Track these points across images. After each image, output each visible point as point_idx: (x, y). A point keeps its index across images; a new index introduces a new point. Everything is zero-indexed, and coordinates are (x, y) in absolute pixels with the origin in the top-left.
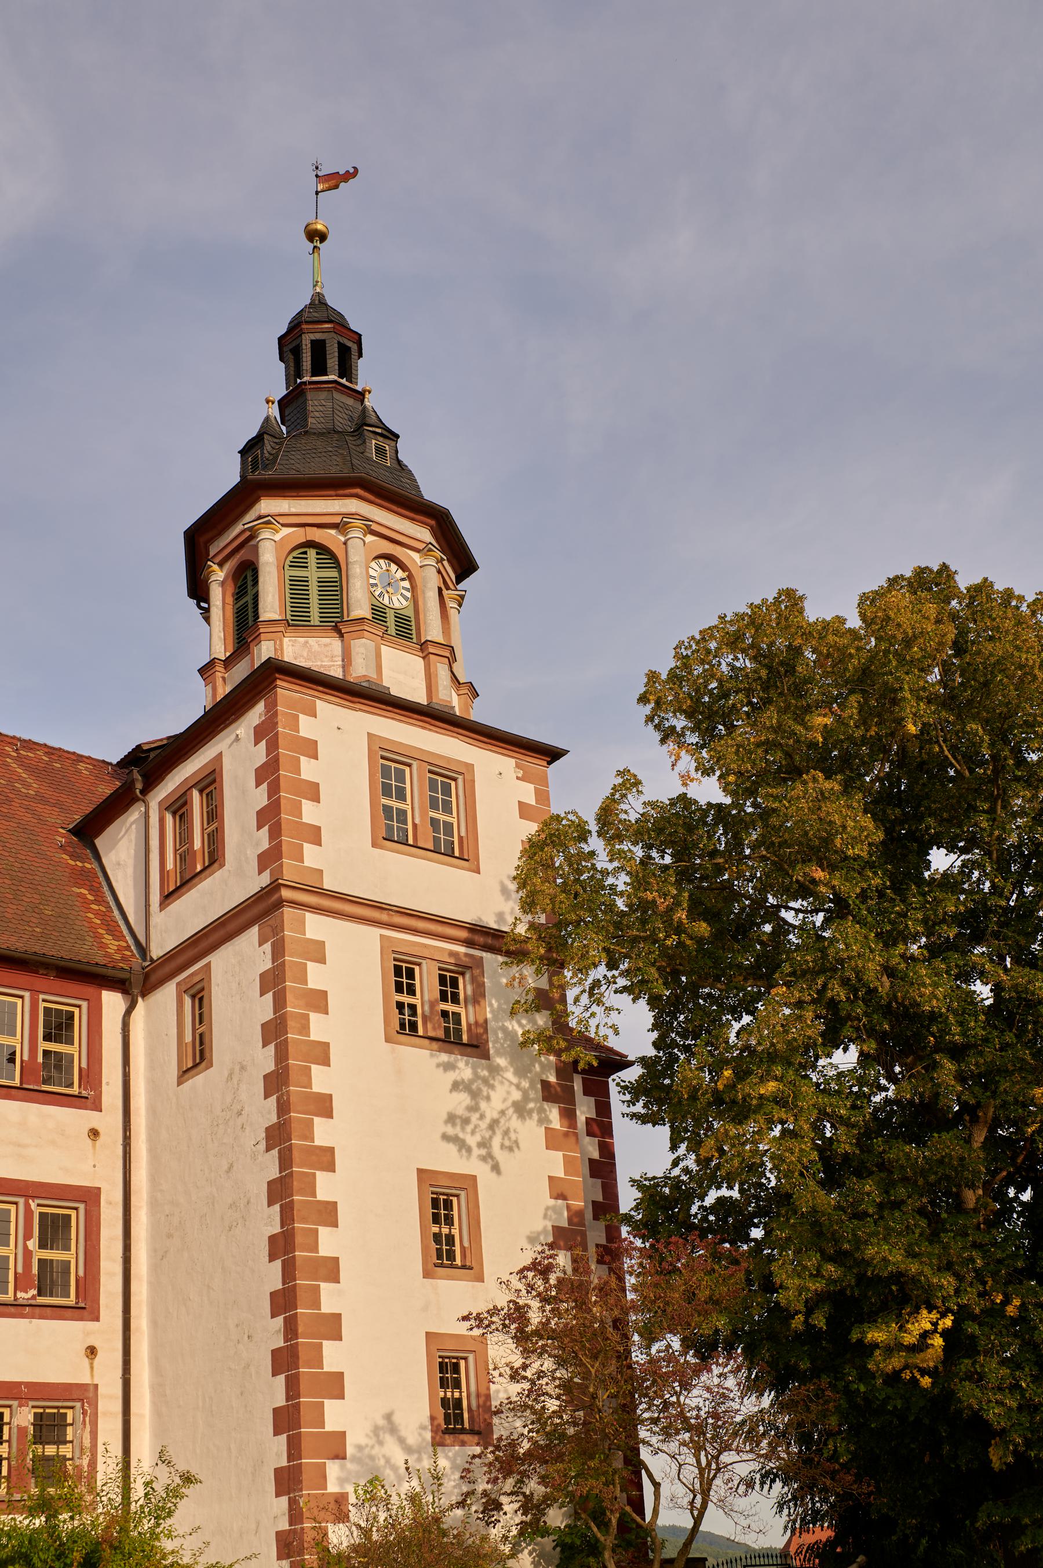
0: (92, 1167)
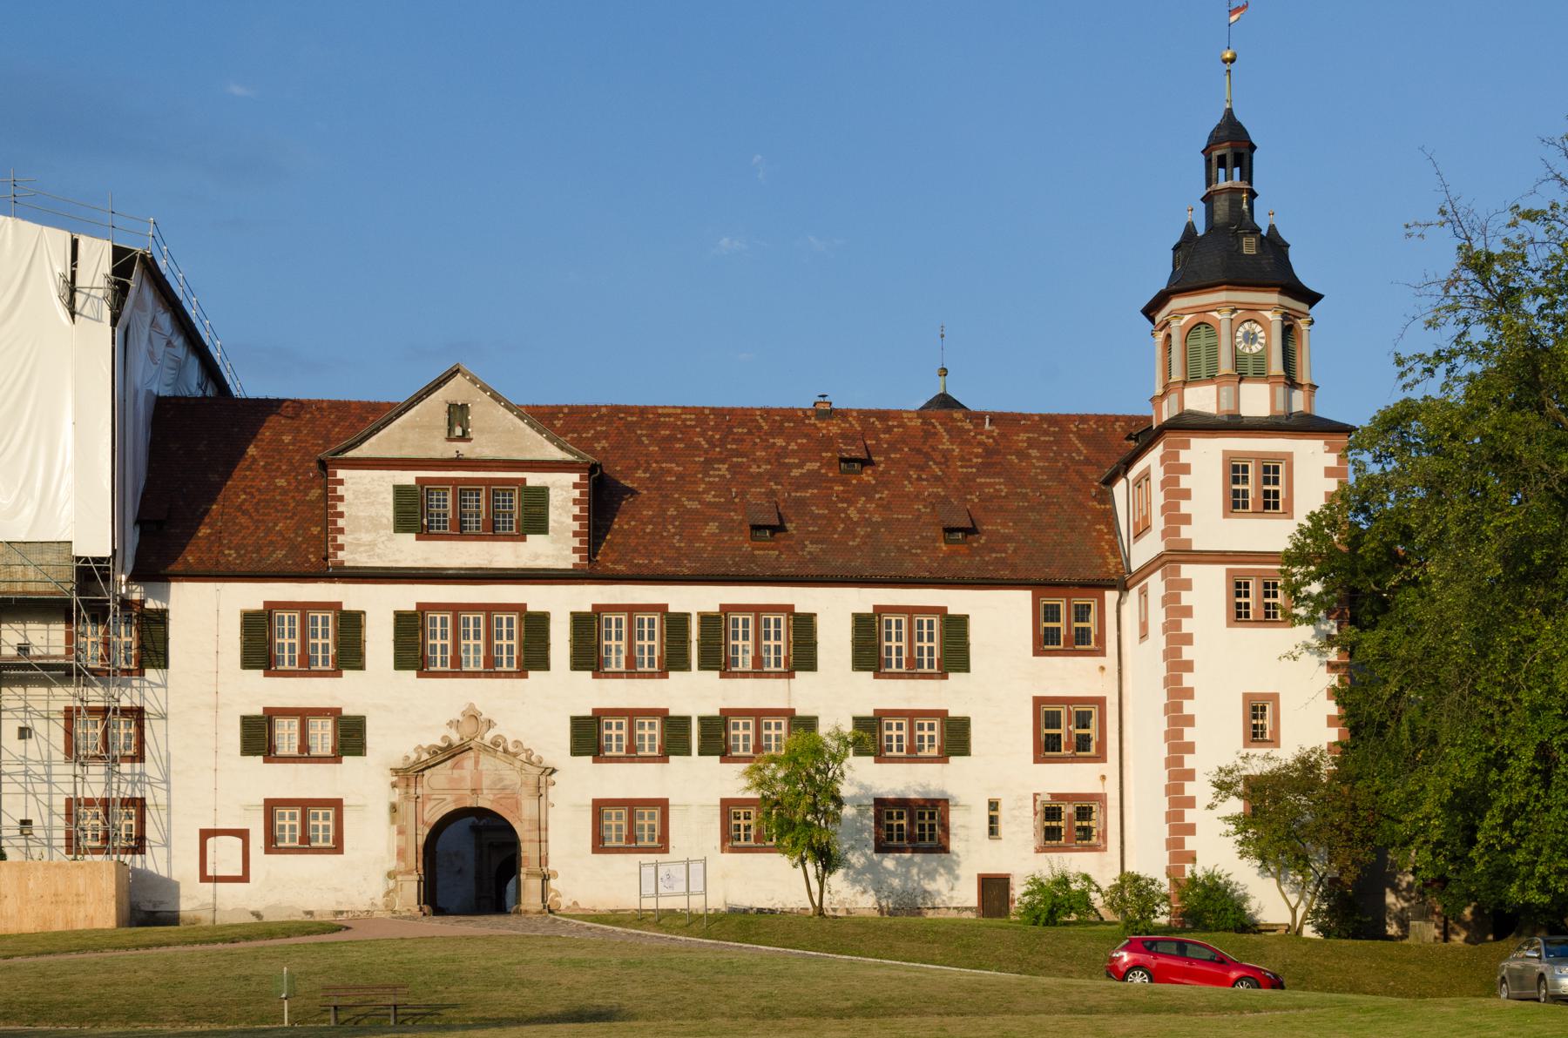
0: (1103, 686)
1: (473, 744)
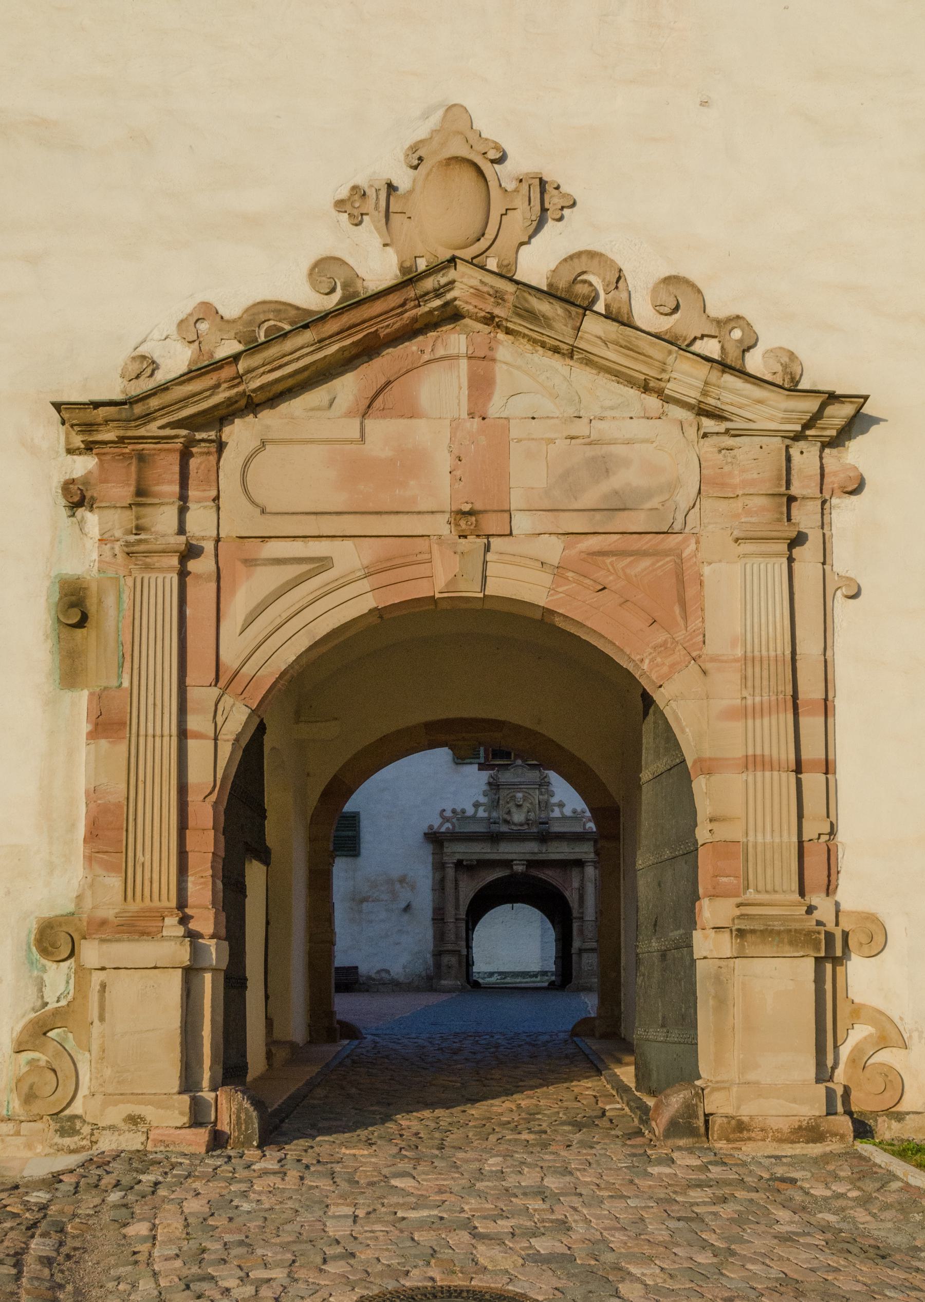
1: (465, 284)
